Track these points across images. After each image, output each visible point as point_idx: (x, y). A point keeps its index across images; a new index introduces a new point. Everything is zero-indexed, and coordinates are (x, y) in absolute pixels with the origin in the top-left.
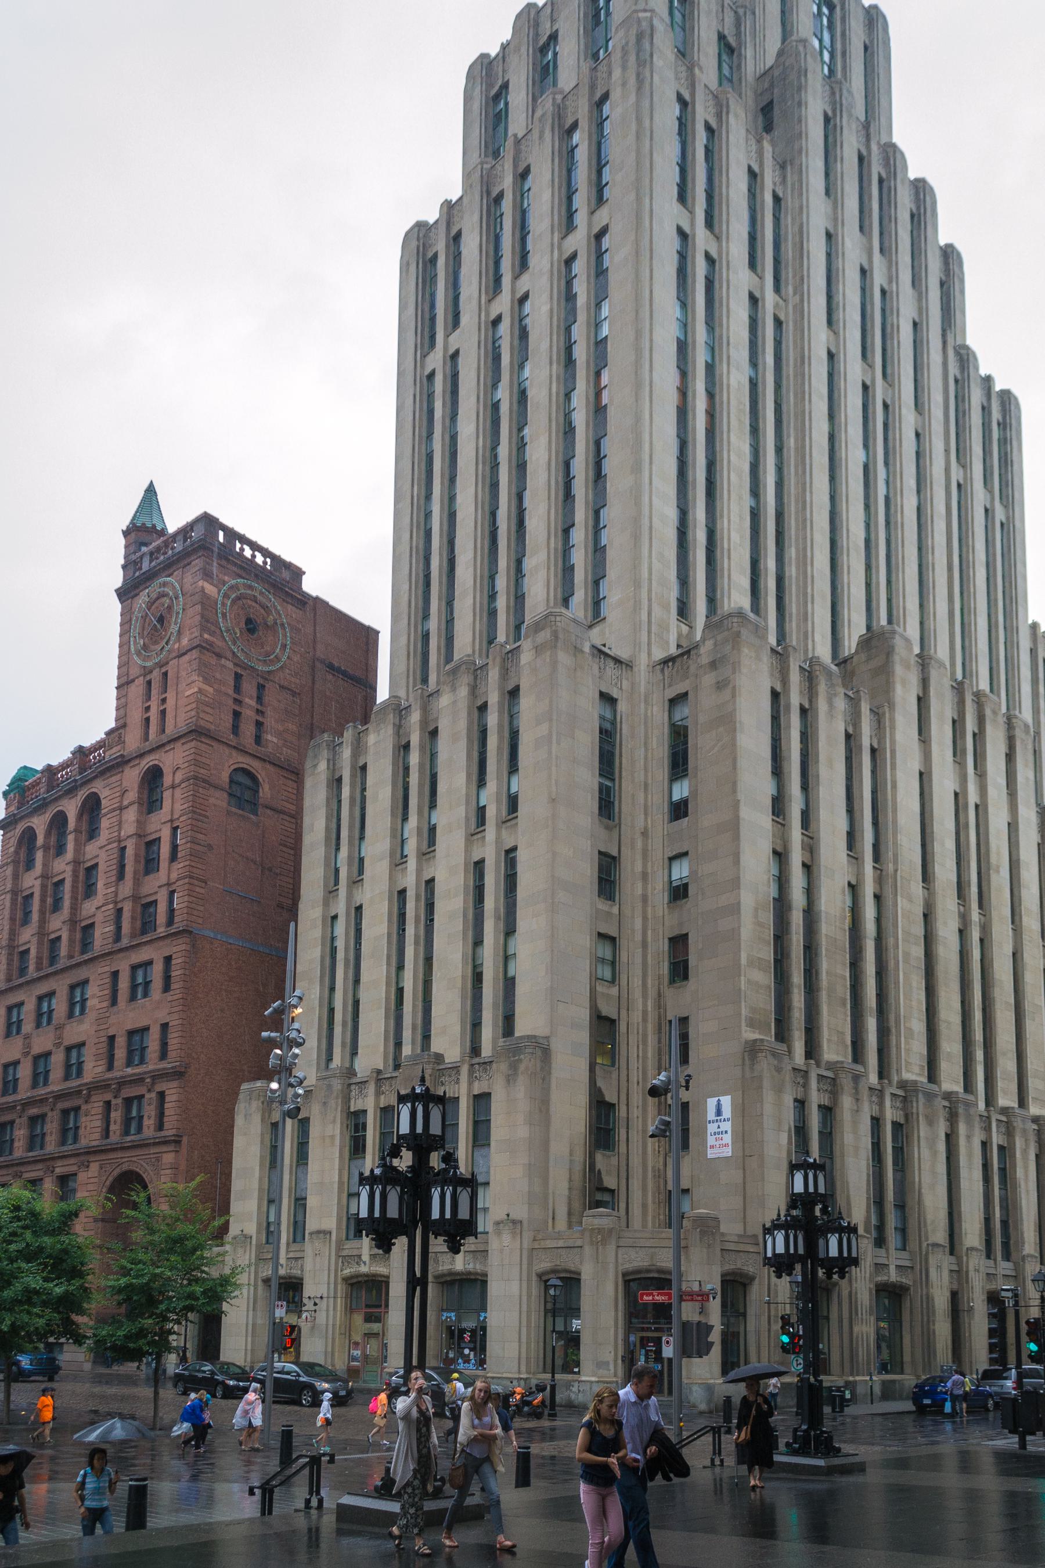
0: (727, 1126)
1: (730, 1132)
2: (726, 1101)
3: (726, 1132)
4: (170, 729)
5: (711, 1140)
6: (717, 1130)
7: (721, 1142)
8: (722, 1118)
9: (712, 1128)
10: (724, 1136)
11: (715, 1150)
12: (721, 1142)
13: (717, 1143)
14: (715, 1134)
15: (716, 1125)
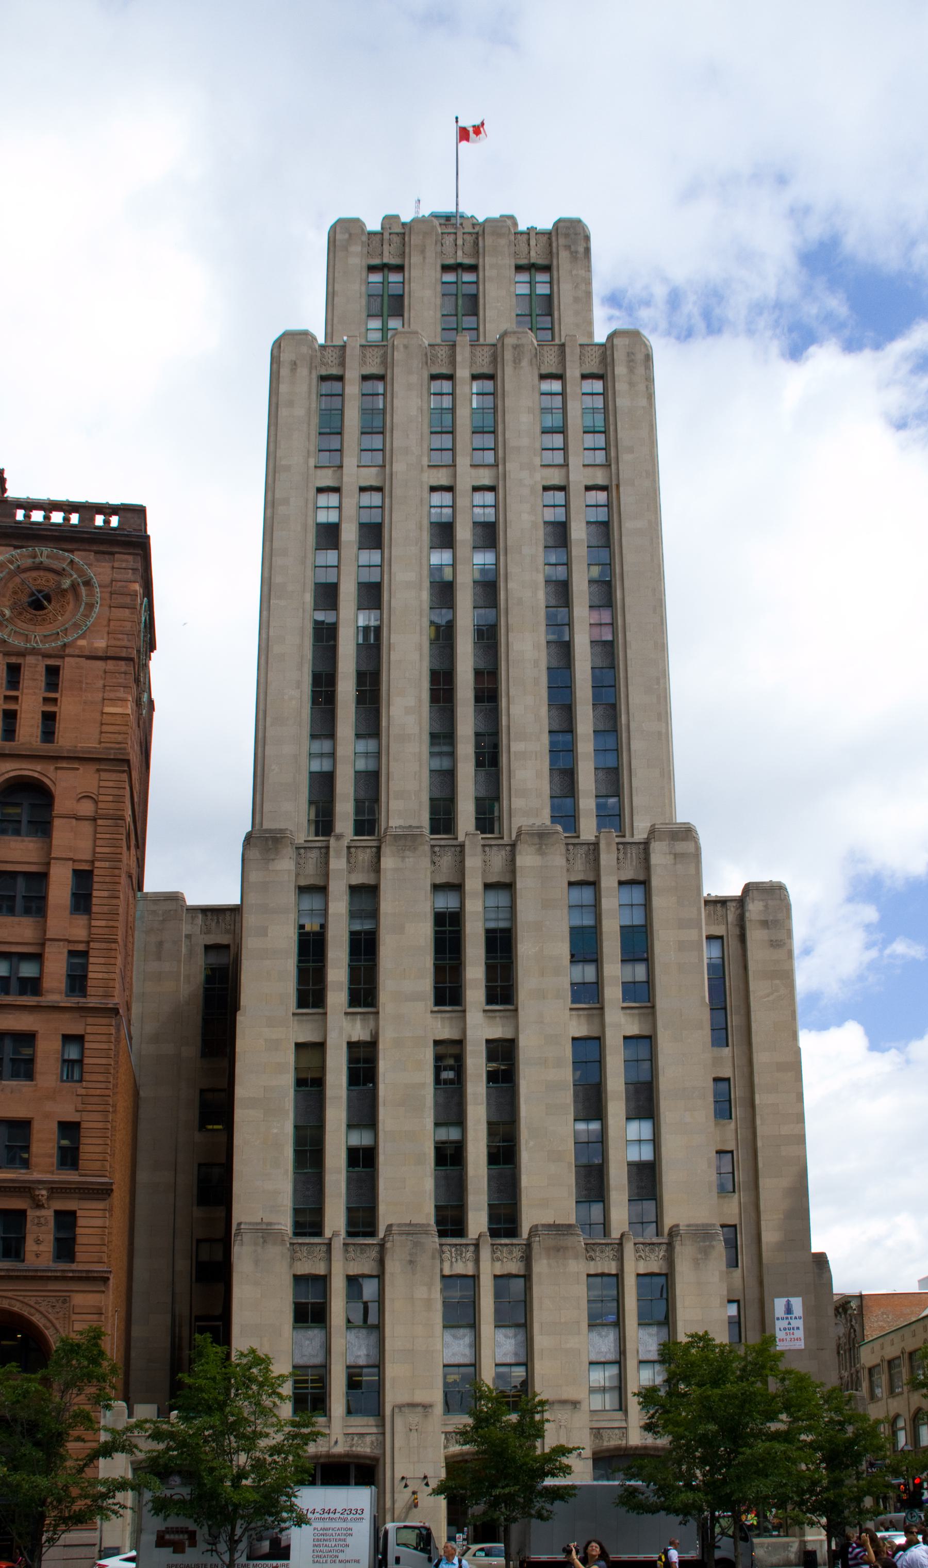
0: (800, 1323)
1: (802, 1328)
2: (797, 1303)
3: (798, 1328)
4: (65, 739)
5: (780, 1335)
6: (787, 1326)
7: (792, 1336)
8: (793, 1316)
9: (779, 1324)
10: (795, 1331)
11: (785, 1343)
12: (792, 1336)
13: (788, 1337)
14: (785, 1329)
15: (786, 1322)
